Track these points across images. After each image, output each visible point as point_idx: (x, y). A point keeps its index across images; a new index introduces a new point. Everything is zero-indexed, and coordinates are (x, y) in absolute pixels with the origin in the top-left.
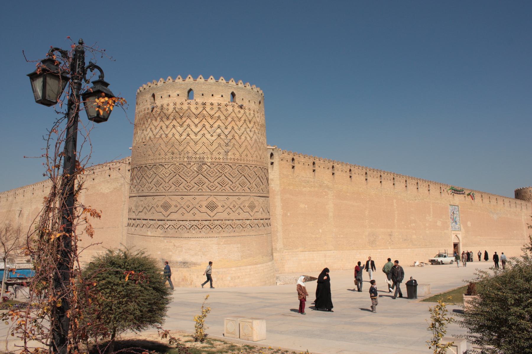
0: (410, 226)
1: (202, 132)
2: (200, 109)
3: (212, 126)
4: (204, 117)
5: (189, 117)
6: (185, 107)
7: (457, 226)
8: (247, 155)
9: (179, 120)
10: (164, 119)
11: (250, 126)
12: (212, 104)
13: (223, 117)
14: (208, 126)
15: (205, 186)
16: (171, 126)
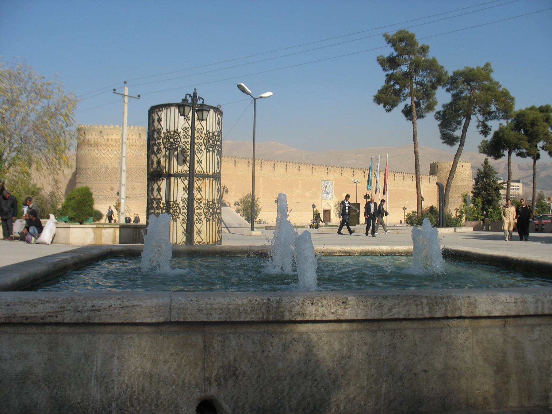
0: (275, 196)
1: (107, 153)
2: (106, 142)
3: (112, 150)
4: (108, 145)
5: (101, 146)
6: (99, 141)
7: (329, 197)
8: (130, 163)
9: (96, 147)
10: (90, 146)
11: (132, 148)
12: (112, 139)
13: (117, 145)
14: (110, 150)
15: (108, 179)
16: (93, 150)
